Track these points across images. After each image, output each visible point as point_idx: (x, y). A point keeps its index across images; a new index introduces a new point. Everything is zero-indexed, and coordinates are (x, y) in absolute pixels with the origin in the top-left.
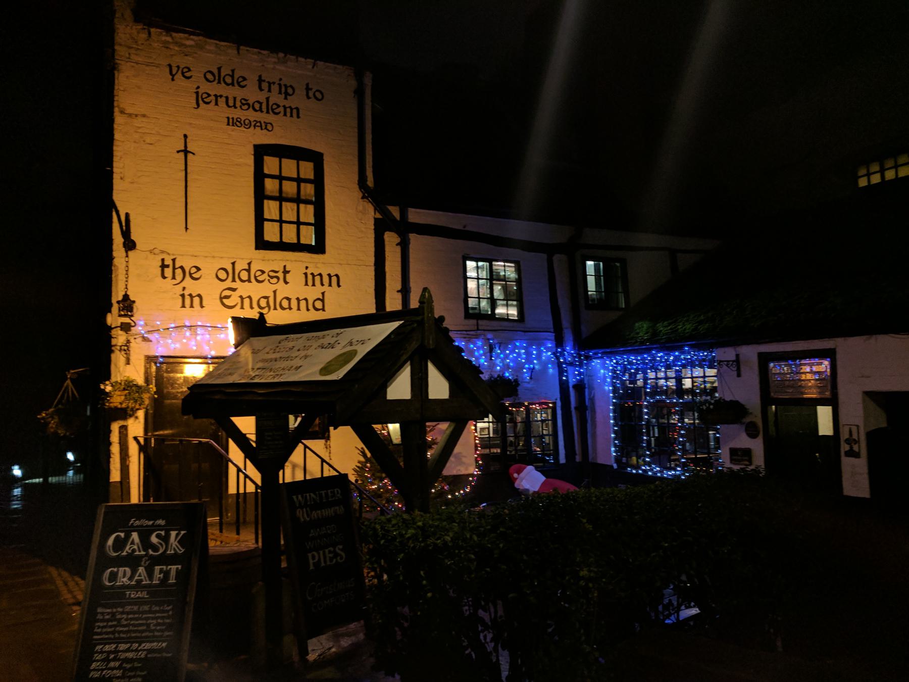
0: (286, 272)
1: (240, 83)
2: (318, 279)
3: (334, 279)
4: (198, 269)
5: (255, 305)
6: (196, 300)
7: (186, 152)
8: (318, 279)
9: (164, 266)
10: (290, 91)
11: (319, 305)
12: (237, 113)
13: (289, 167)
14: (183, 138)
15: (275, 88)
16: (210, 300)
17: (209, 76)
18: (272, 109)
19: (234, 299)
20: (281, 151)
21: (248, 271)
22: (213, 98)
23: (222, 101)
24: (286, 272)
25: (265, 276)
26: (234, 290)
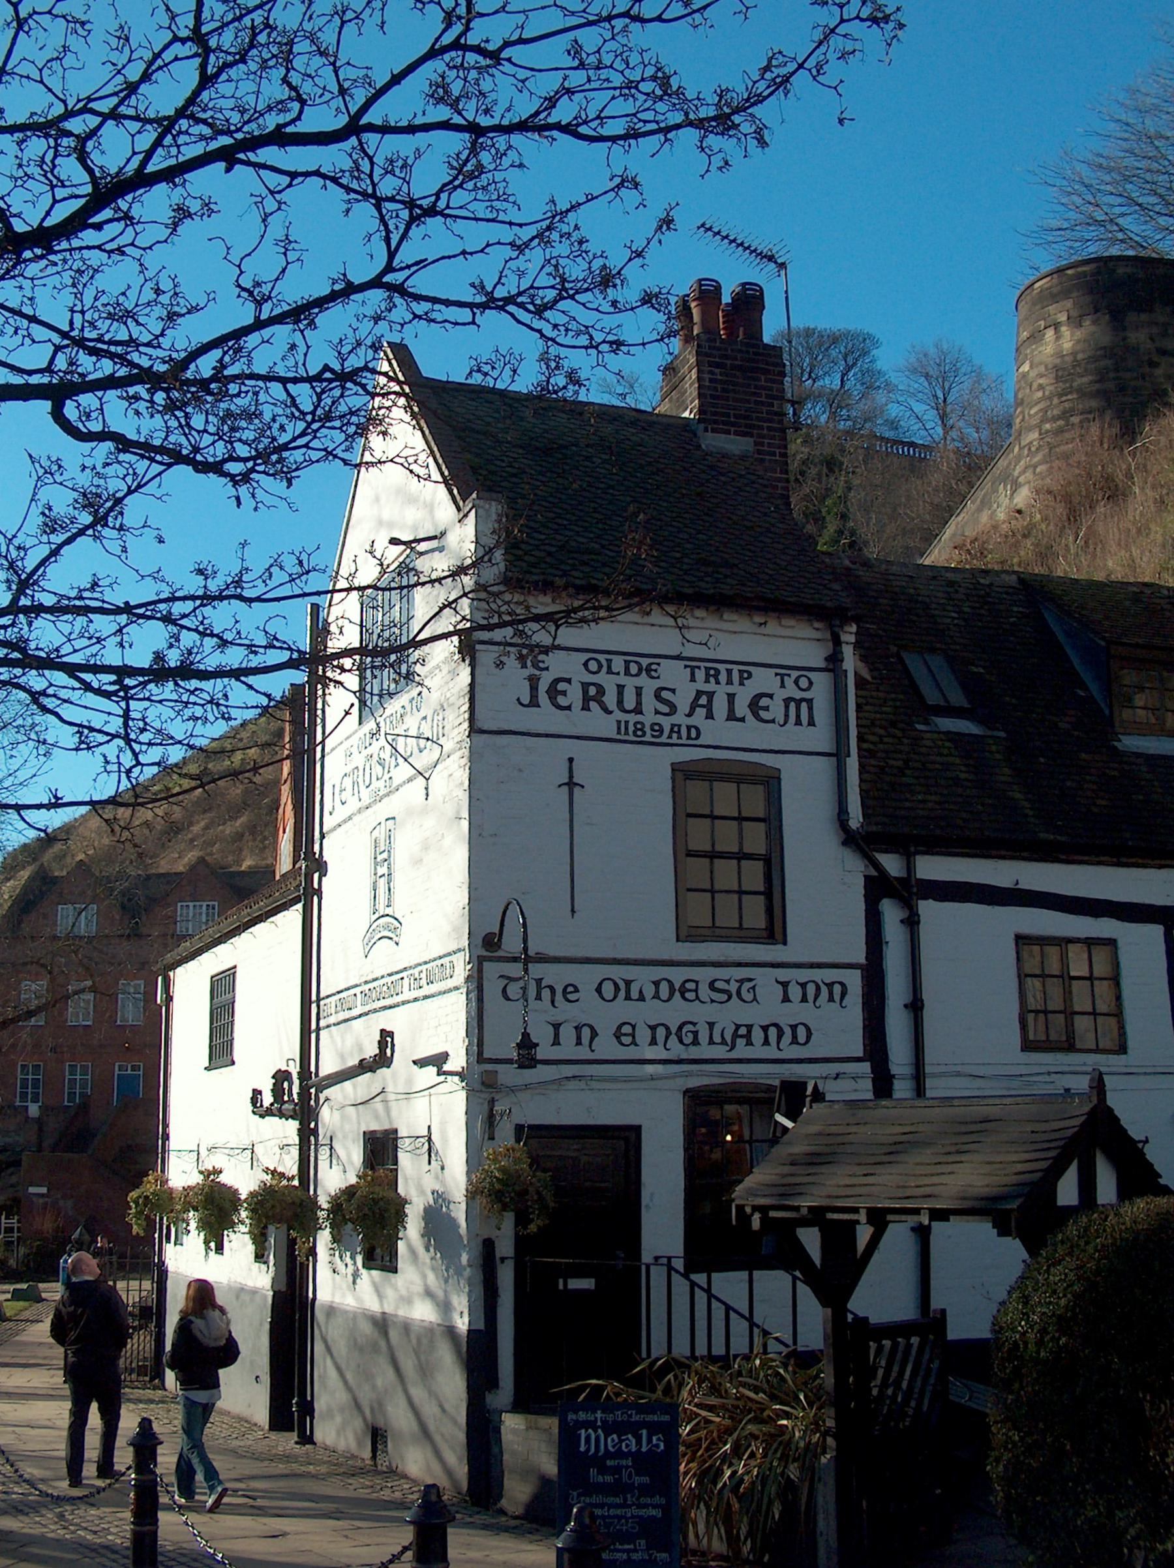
7: (571, 784)
13: (725, 798)
14: (567, 764)
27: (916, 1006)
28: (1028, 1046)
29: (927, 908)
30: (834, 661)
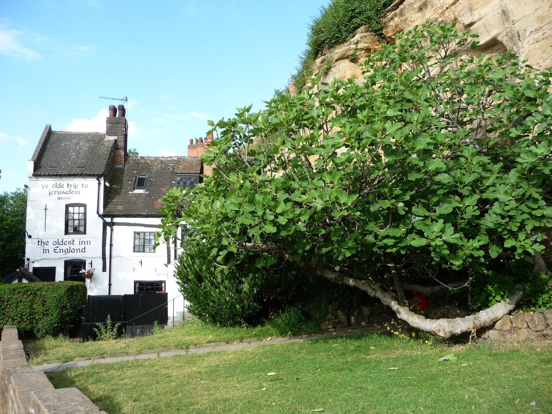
0: (73, 241)
1: (61, 186)
2: (83, 243)
3: (89, 243)
4: (48, 242)
5: (64, 251)
6: (47, 251)
8: (83, 243)
9: (39, 242)
10: (77, 186)
11: (83, 250)
12: (60, 196)
13: (76, 209)
15: (72, 186)
16: (51, 251)
17: (53, 186)
18: (71, 192)
19: (58, 250)
20: (74, 205)
21: (62, 242)
22: (54, 192)
23: (57, 193)
24: (73, 241)
25: (67, 243)
26: (58, 247)
27: (111, 245)
28: (134, 251)
29: (115, 227)
30: (99, 184)
